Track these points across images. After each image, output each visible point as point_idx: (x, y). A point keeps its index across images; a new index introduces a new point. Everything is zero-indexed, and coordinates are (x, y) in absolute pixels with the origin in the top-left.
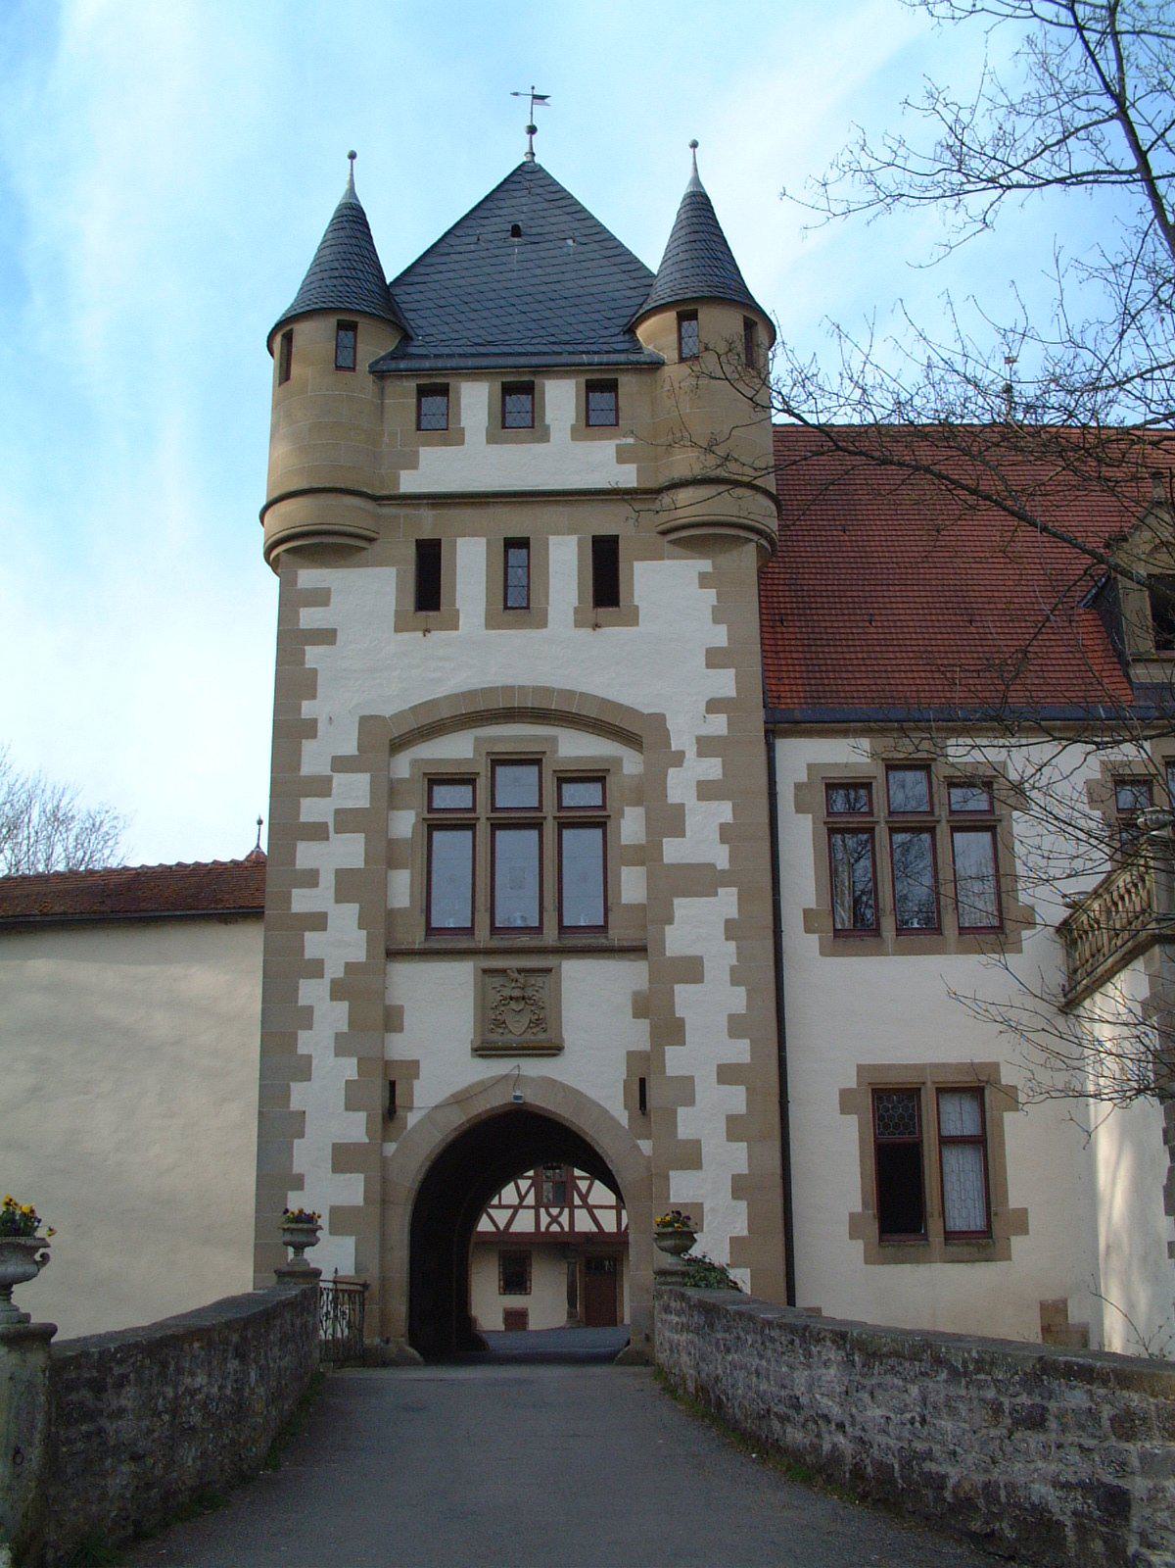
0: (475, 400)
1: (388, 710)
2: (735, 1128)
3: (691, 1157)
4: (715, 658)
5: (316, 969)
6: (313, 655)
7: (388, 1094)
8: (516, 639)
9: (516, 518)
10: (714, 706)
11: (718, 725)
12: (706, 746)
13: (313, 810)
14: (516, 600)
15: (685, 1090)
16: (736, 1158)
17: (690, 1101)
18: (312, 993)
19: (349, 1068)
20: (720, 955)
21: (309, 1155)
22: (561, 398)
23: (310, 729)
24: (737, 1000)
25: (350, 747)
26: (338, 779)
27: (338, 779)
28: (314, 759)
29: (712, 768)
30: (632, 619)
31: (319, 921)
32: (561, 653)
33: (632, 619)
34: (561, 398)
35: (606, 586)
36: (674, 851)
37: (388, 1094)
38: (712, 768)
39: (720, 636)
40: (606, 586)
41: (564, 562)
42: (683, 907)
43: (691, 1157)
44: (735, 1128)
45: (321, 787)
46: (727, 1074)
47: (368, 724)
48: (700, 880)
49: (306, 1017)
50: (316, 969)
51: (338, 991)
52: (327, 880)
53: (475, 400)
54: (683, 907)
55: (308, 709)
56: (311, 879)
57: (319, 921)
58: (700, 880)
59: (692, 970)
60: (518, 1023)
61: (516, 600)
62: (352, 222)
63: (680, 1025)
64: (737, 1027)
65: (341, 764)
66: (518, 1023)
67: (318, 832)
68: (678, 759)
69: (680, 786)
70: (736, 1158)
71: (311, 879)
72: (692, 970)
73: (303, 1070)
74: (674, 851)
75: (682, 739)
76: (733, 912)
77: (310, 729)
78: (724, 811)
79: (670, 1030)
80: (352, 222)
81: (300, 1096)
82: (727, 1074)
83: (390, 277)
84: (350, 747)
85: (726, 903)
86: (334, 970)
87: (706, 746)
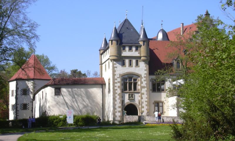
0: (127, 49)
1: (121, 73)
2: (146, 105)
3: (143, 107)
4: (145, 70)
5: (117, 93)
6: (115, 69)
7: (123, 102)
8: (131, 68)
9: (131, 58)
10: (145, 74)
11: (145, 75)
12: (145, 77)
13: (116, 81)
14: (130, 64)
15: (143, 102)
16: (146, 107)
17: (143, 103)
18: (116, 95)
19: (119, 101)
20: (145, 93)
21: (117, 106)
22: (134, 49)
23: (115, 75)
24: (146, 96)
25: (119, 76)
26: (117, 78)
27: (118, 79)
28: (116, 77)
29: (145, 79)
30: (139, 67)
31: (117, 90)
32: (133, 70)
33: (139, 67)
34: (134, 49)
35: (137, 64)
36: (142, 85)
37: (123, 102)
38: (145, 79)
39: (146, 68)
40: (137, 64)
41: (134, 61)
42: (143, 89)
43: (143, 107)
44: (146, 105)
45: (116, 79)
46: (146, 101)
47: (120, 74)
48: (144, 87)
49: (116, 97)
50: (117, 93)
51: (118, 95)
52: (117, 87)
53: (127, 49)
54: (143, 89)
55: (115, 73)
56: (116, 86)
57: (117, 90)
58: (144, 87)
59: (143, 94)
60: (131, 97)
61: (130, 64)
62: (115, 28)
63: (142, 98)
64: (146, 98)
65: (118, 78)
66: (131, 97)
67: (116, 83)
68: (142, 78)
69: (143, 80)
70: (146, 107)
71: (116, 86)
72: (143, 94)
73: (116, 101)
74: (142, 85)
75: (143, 76)
76: (146, 90)
77: (115, 75)
78: (146, 82)
79: (142, 98)
80: (115, 28)
81: (116, 103)
82: (146, 101)
83: (118, 32)
84: (119, 76)
85: (146, 89)
86: (118, 93)
87: (145, 77)
